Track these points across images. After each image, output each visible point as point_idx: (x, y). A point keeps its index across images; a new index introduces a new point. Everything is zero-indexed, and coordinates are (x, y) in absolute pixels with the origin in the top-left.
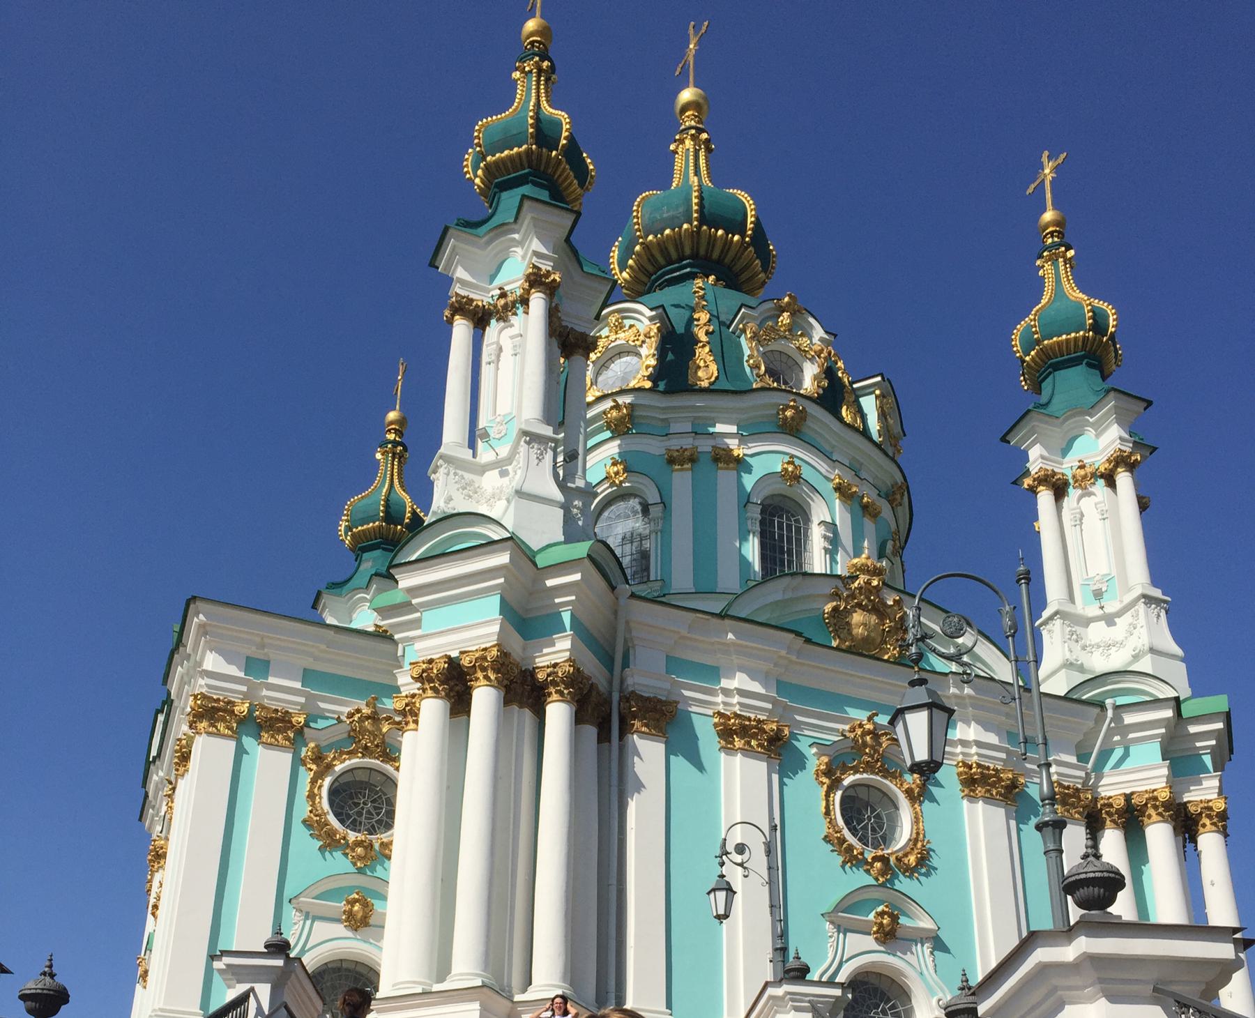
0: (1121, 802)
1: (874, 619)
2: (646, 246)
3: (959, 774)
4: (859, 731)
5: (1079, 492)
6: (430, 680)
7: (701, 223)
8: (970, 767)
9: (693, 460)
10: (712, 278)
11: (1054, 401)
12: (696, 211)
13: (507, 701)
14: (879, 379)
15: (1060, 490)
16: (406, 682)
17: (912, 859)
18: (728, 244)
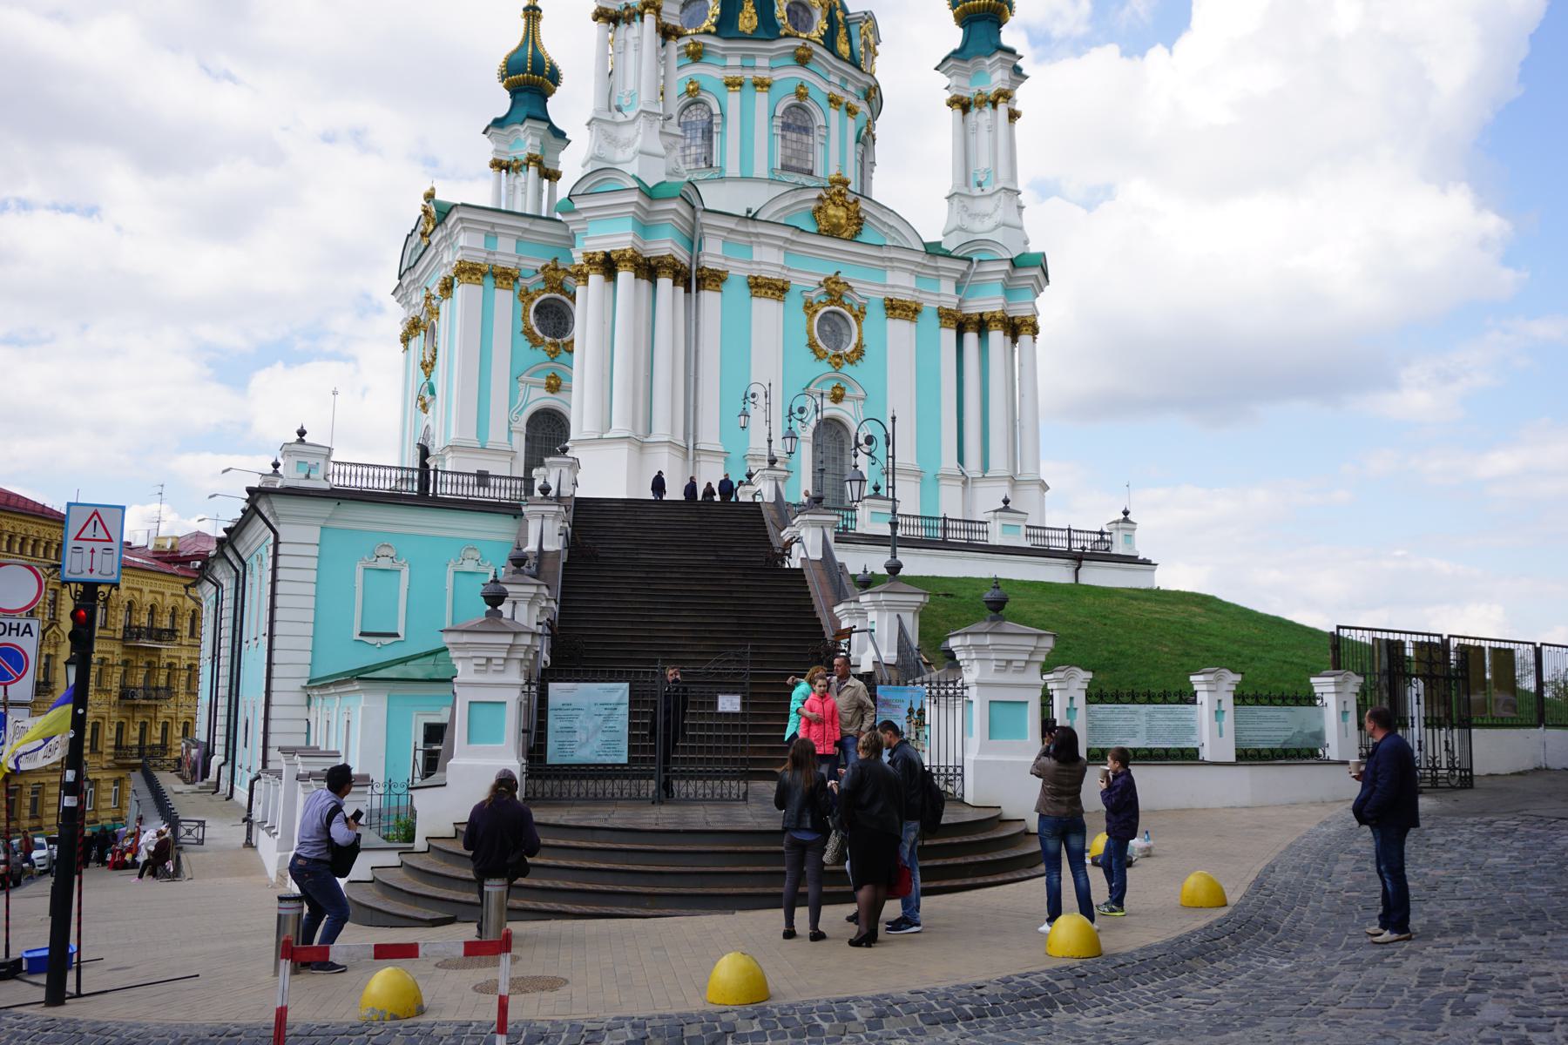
1: (841, 213)
9: (741, 85)
16: (578, 259)
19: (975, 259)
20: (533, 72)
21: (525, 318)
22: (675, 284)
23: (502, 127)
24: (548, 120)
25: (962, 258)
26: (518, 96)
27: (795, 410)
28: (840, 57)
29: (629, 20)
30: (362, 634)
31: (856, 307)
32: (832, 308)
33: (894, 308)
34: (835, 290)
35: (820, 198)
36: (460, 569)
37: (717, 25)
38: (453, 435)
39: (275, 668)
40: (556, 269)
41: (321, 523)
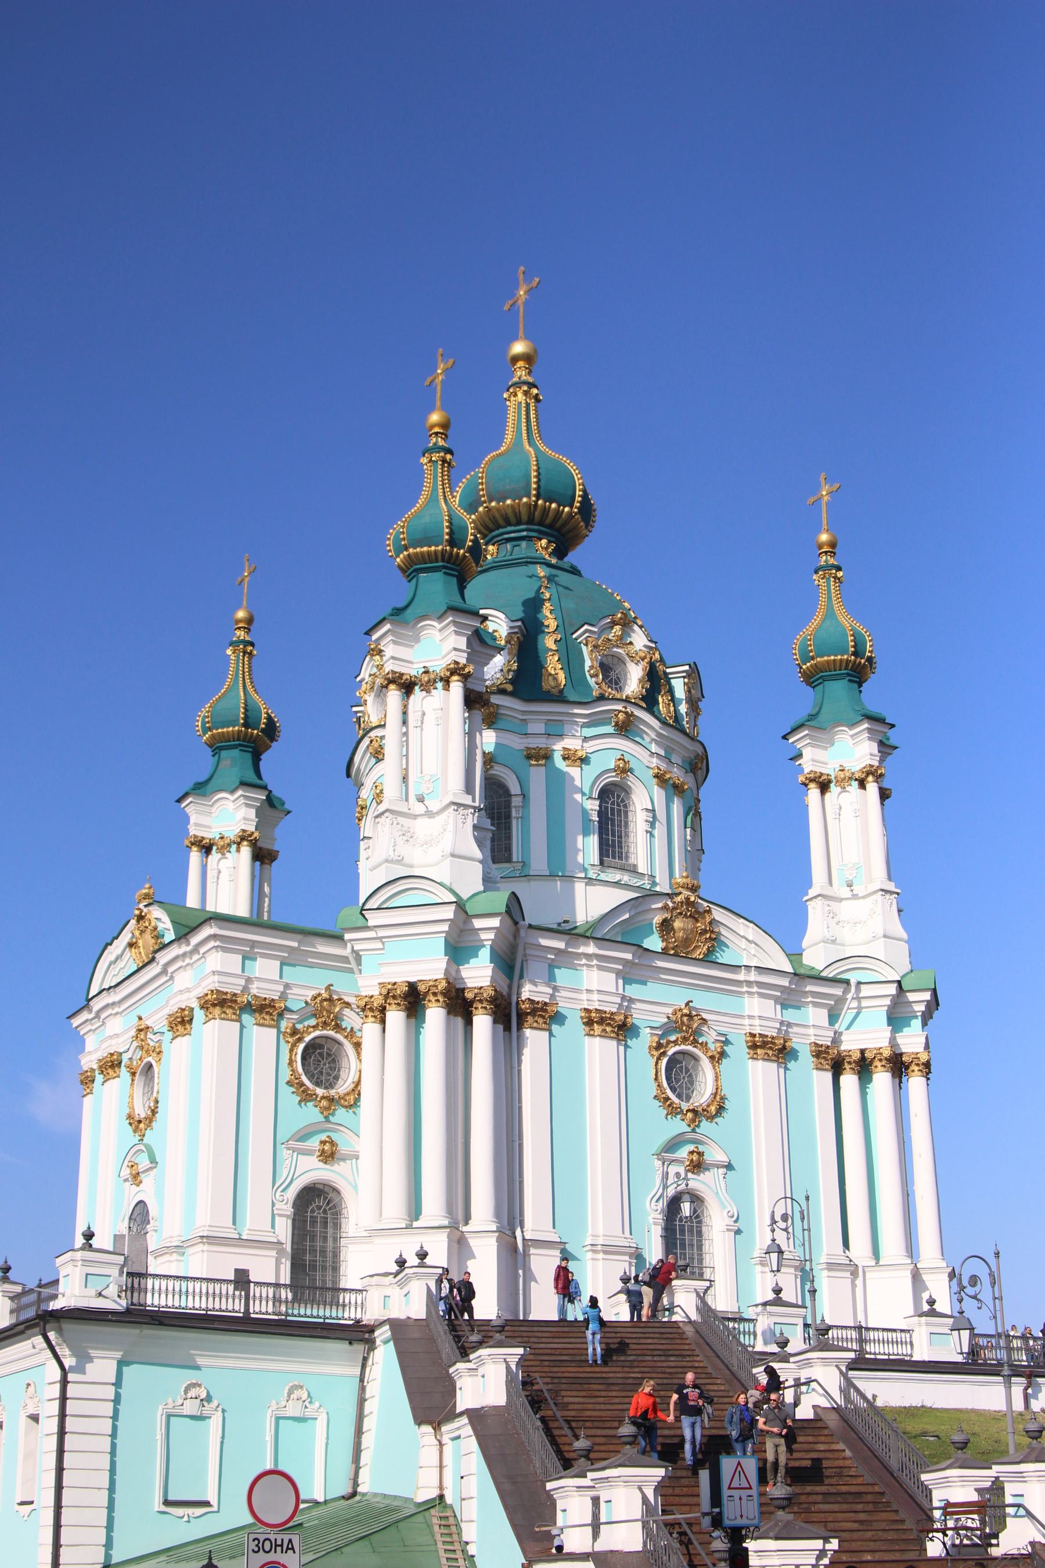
0: (857, 1056)
2: (489, 510)
3: (747, 1042)
4: (679, 1014)
5: (839, 789)
6: (394, 997)
7: (538, 497)
8: (753, 1035)
10: (544, 542)
11: (823, 711)
12: (535, 489)
13: (449, 1013)
14: (687, 668)
15: (824, 787)
17: (713, 1109)
18: (558, 514)
19: (853, 977)
20: (246, 725)
21: (291, 1063)
22: (495, 1022)
23: (204, 795)
24: (265, 788)
25: (834, 981)
26: (224, 753)
27: (778, 1218)
28: (664, 723)
29: (428, 687)
30: (167, 1503)
31: (711, 1046)
32: (683, 1047)
33: (759, 1045)
34: (687, 1024)
35: (665, 908)
36: (282, 1413)
37: (512, 682)
38: (203, 1223)
39: (63, 1551)
40: (330, 1000)
41: (118, 1355)
